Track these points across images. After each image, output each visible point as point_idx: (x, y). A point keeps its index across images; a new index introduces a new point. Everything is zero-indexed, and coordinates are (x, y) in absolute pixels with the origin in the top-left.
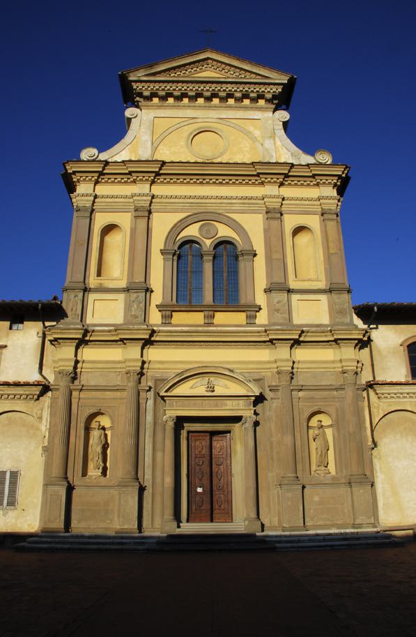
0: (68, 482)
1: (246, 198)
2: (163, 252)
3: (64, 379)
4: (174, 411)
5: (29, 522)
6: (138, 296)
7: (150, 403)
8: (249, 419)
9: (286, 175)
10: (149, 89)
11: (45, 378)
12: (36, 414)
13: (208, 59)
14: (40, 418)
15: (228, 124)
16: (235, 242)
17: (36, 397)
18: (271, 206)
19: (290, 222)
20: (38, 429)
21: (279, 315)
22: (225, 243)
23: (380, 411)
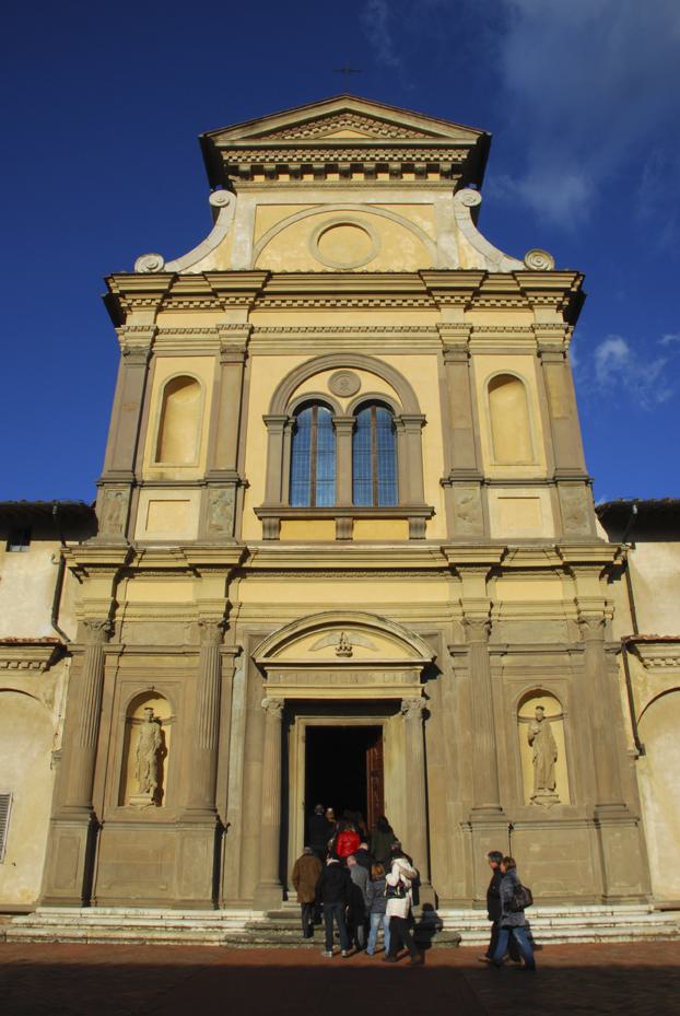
0: (93, 816)
1: (409, 329)
2: (267, 421)
3: (93, 634)
4: (280, 689)
5: (23, 887)
6: (224, 494)
7: (241, 676)
8: (413, 705)
9: (476, 290)
10: (249, 160)
11: (61, 633)
12: (45, 694)
14: (51, 702)
15: (379, 212)
16: (391, 403)
17: (44, 665)
18: (451, 341)
19: (485, 367)
20: (47, 721)
21: (466, 523)
23: (648, 688)
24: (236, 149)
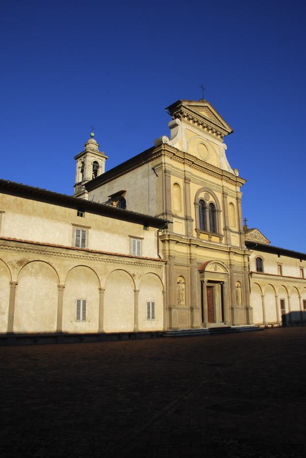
9: (222, 175)
13: (207, 107)
22: (212, 204)
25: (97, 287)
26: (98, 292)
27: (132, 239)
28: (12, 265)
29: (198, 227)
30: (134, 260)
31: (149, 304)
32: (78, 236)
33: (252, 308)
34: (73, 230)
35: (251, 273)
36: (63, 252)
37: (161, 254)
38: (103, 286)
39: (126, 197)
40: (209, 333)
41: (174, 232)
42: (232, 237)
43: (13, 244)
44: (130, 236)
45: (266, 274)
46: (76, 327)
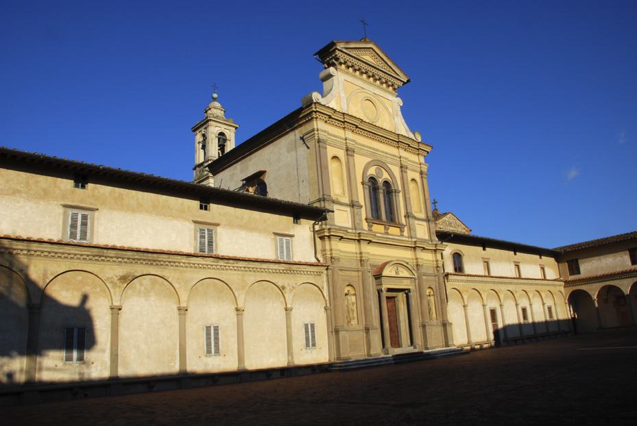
9: (398, 141)
13: (371, 48)
22: (386, 183)
24: (342, 51)
25: (234, 307)
26: (234, 313)
27: (278, 237)
28: (112, 282)
29: (370, 216)
30: (282, 267)
31: (306, 326)
32: (202, 237)
33: (451, 324)
34: (195, 229)
35: (447, 275)
36: (183, 261)
37: (319, 256)
38: (240, 306)
39: (267, 179)
40: (393, 362)
41: (336, 224)
42: (417, 226)
43: (112, 253)
44: (276, 234)
45: (468, 275)
46: (206, 365)
